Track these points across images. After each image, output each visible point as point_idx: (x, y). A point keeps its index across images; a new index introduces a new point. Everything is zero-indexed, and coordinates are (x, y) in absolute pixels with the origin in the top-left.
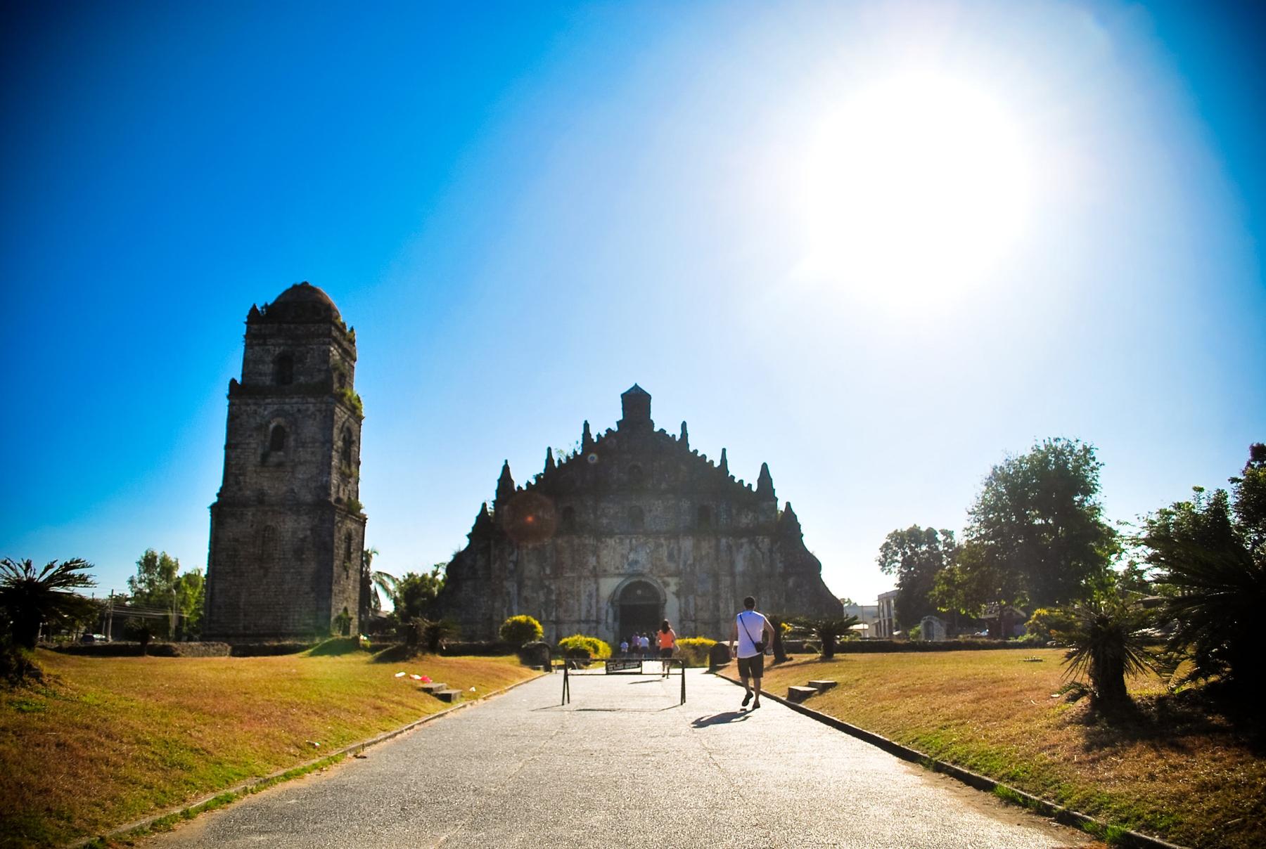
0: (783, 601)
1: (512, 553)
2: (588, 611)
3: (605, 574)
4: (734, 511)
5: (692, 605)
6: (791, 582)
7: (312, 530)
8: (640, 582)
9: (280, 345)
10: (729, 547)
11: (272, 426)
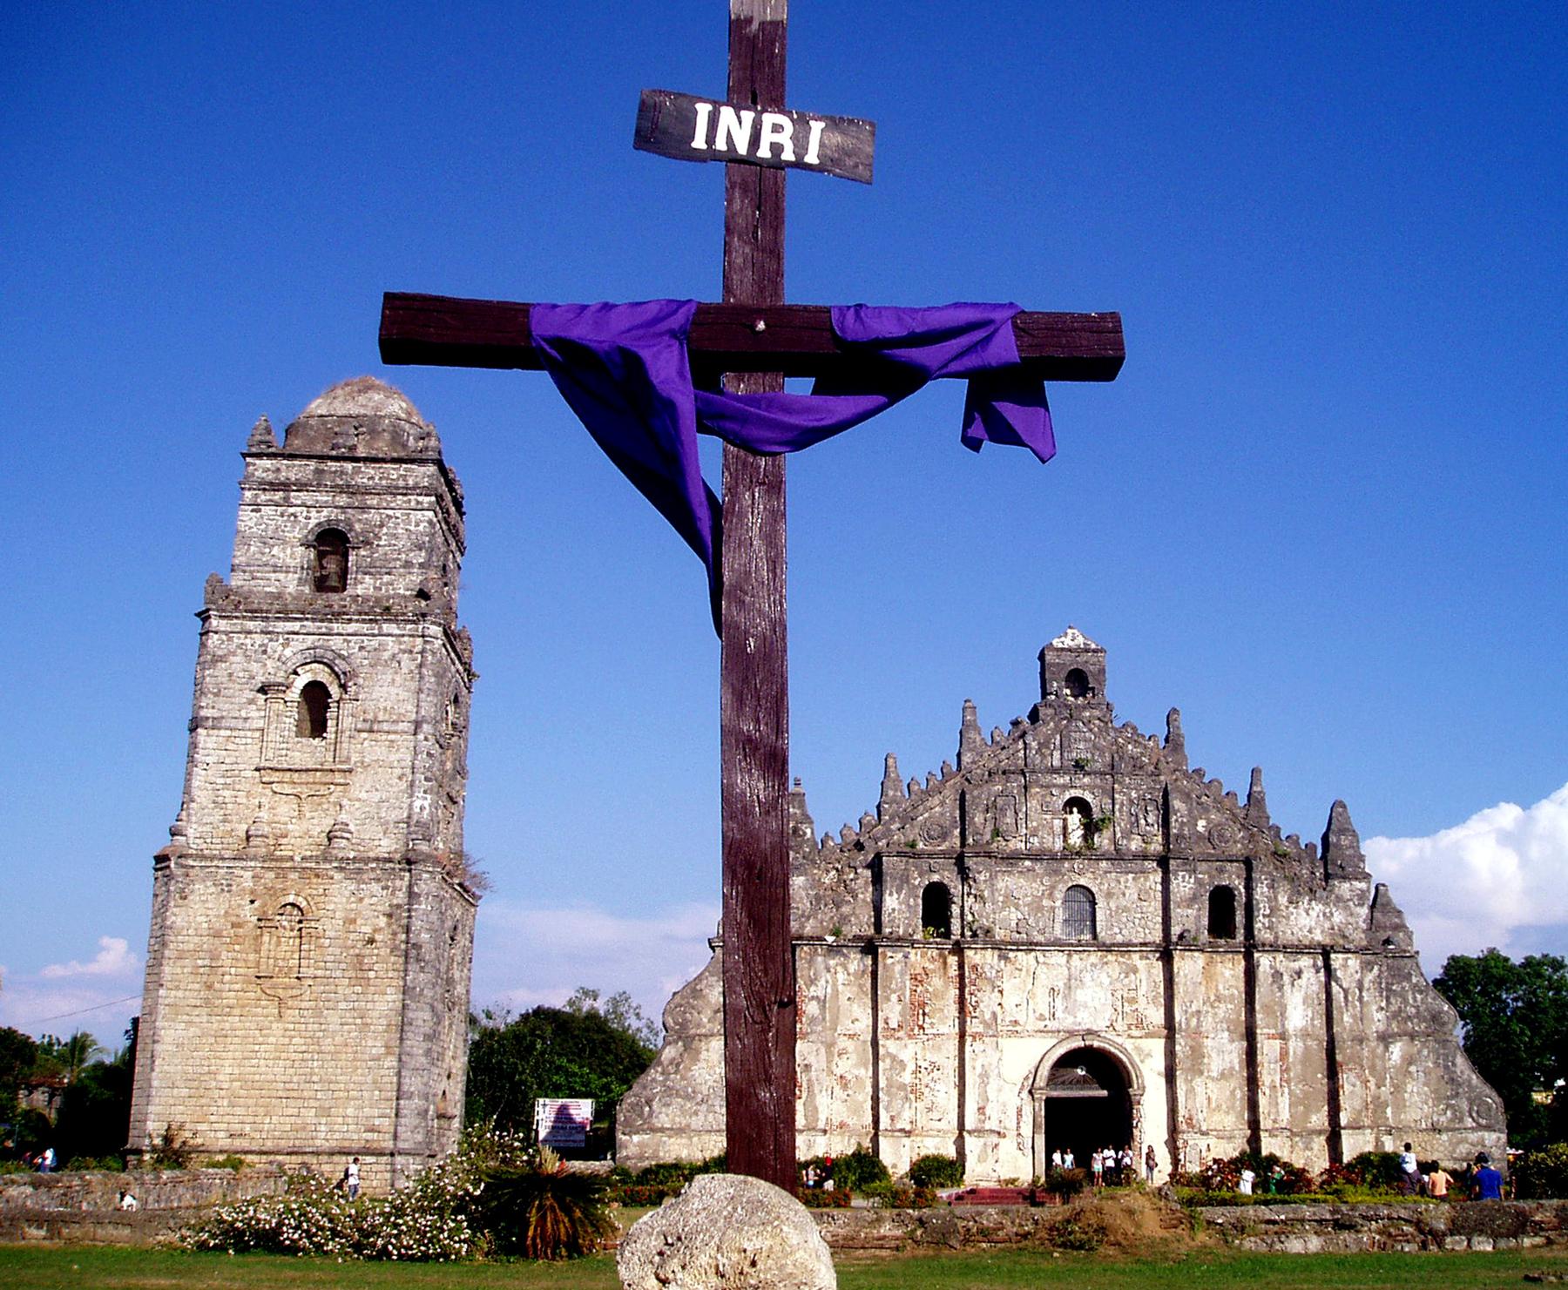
0: (1385, 1090)
1: (812, 982)
2: (981, 1110)
3: (1015, 1029)
4: (1283, 900)
5: (1201, 1100)
6: (1397, 1051)
7: (390, 916)
8: (1089, 1050)
9: (319, 507)
10: (1277, 975)
11: (300, 682)
